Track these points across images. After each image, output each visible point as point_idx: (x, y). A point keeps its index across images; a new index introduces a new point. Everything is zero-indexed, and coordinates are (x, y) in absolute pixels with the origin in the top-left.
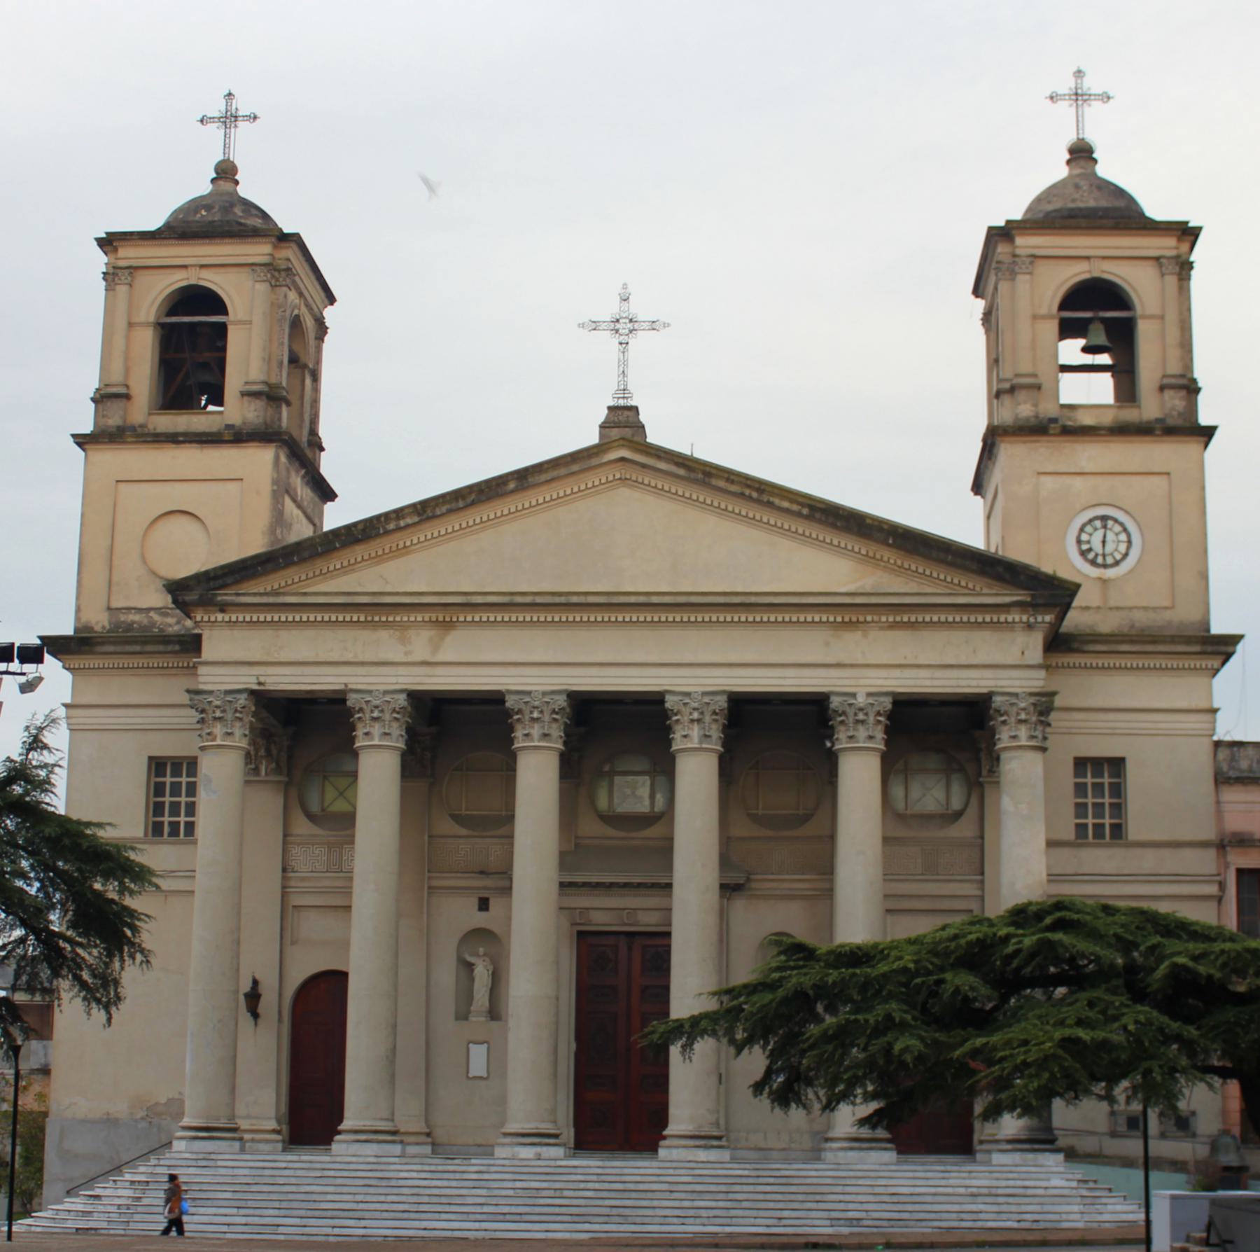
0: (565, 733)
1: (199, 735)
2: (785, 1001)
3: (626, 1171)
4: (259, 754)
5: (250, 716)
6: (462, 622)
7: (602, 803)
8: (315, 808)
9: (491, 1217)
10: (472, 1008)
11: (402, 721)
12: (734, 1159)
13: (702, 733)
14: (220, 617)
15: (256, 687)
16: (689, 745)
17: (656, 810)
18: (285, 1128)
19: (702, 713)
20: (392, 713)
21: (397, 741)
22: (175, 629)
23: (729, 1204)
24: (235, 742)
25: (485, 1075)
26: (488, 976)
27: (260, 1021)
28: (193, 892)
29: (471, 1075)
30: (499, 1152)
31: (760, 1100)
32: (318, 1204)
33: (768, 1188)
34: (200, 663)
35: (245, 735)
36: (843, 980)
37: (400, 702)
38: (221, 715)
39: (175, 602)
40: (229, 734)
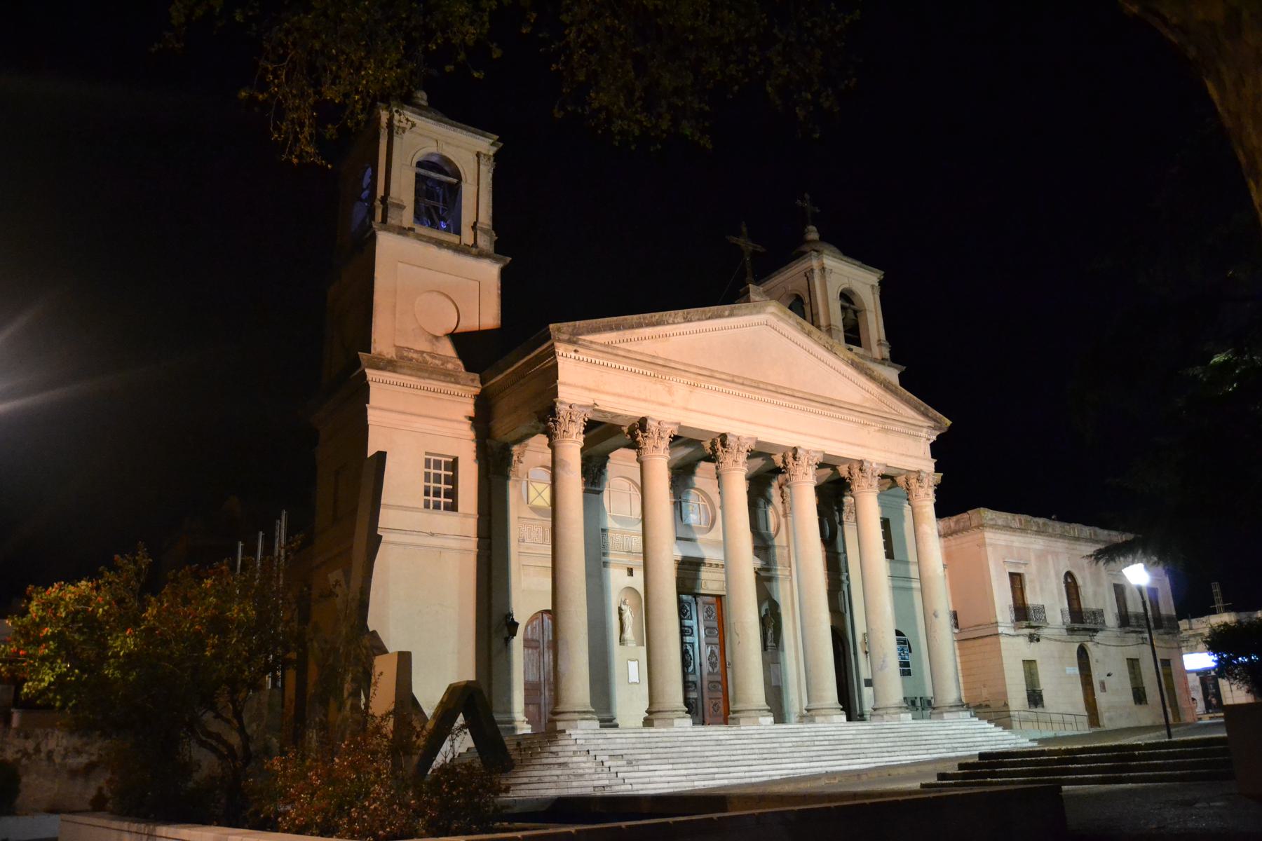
14: (573, 354)
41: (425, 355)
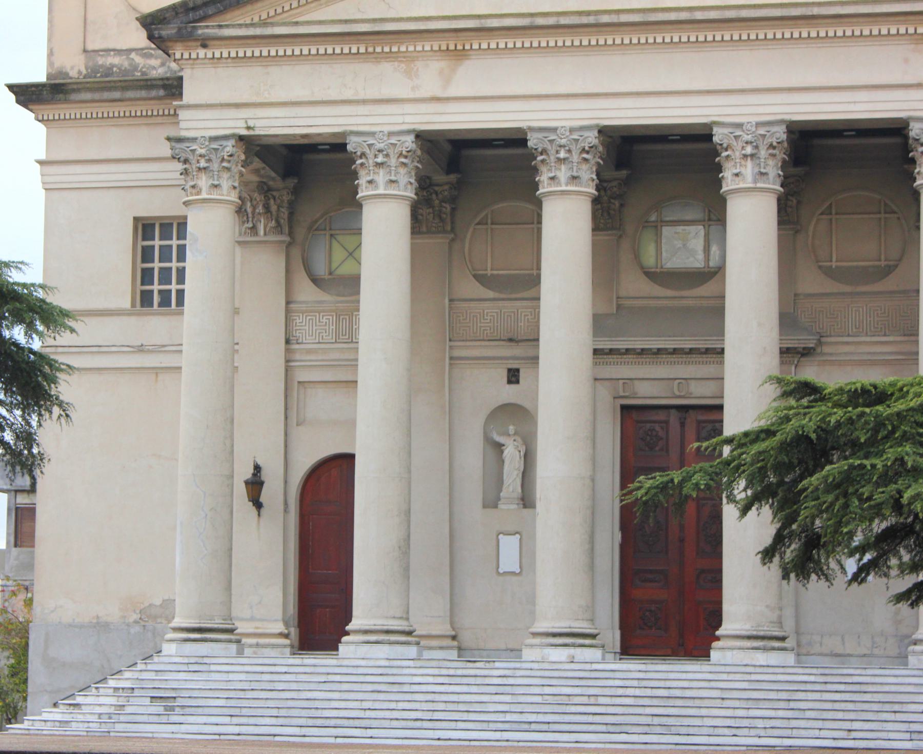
0: (598, 175)
1: (183, 189)
2: (784, 447)
3: (672, 676)
4: (257, 211)
5: (240, 165)
6: (476, 50)
7: (649, 258)
8: (321, 270)
9: (515, 726)
10: (501, 494)
11: (411, 166)
12: (799, 663)
13: (757, 170)
14: (202, 52)
15: (244, 132)
16: (742, 185)
17: (711, 264)
18: (294, 632)
19: (757, 147)
20: (398, 157)
21: (406, 189)
22: (160, 72)
23: (789, 714)
24: (223, 195)
25: (518, 571)
26: (520, 458)
27: (263, 511)
28: (180, 368)
29: (501, 571)
30: (528, 654)
31: (769, 568)
32: (320, 711)
33: (837, 697)
34: (181, 107)
35: (235, 188)
36: (851, 421)
37: (407, 144)
38: (206, 165)
39: (151, 38)
40: (216, 186)
41: (133, 55)
